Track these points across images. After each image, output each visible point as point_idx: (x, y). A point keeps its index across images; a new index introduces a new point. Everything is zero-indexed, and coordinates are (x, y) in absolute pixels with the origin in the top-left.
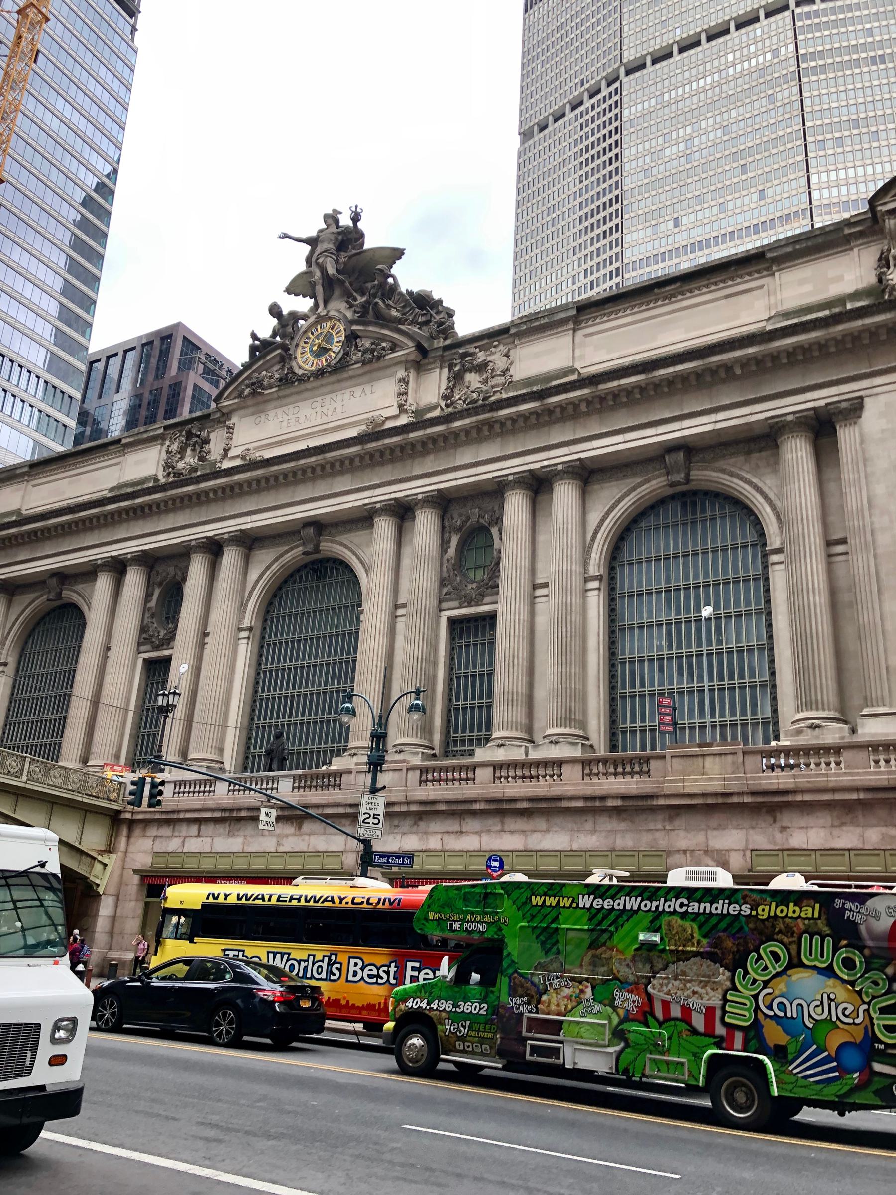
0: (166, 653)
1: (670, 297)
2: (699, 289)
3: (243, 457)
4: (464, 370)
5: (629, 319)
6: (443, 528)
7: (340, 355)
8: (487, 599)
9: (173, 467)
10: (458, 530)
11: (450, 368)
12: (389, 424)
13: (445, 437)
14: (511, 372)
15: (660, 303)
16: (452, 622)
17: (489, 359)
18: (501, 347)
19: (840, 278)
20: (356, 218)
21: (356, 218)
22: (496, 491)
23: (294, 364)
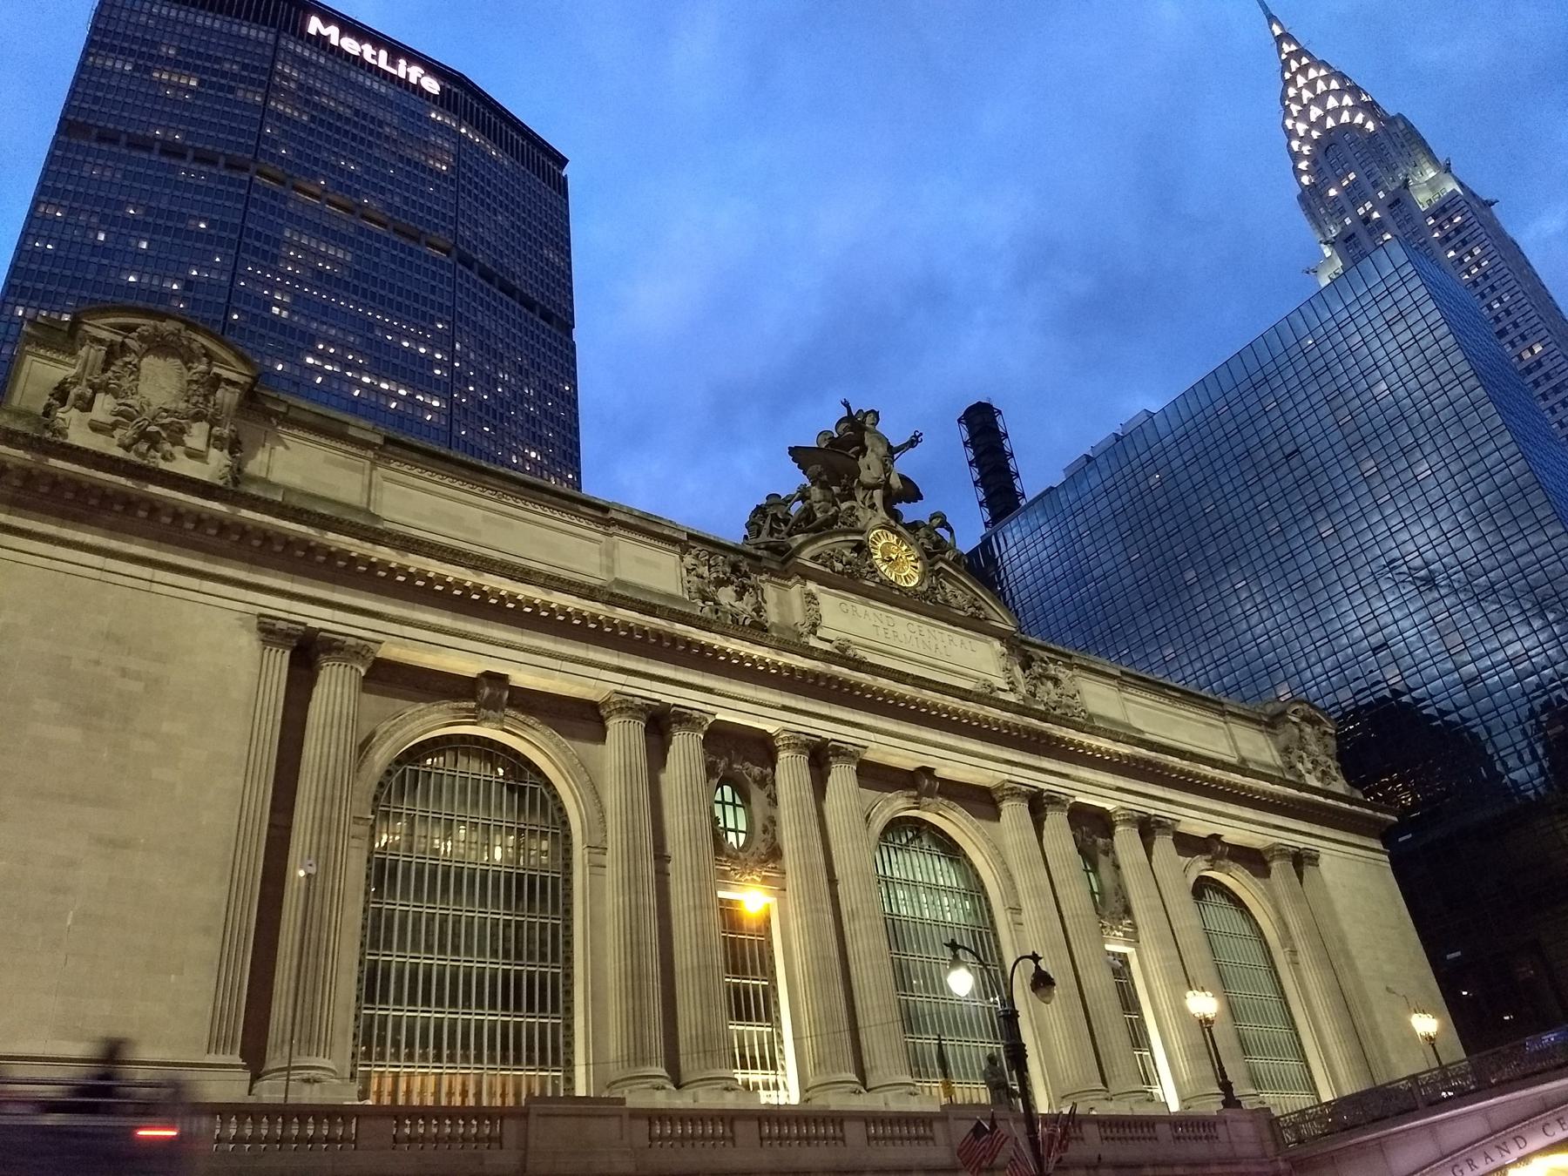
3: (843, 649)
7: (925, 587)
9: (717, 603)
17: (1061, 676)
20: (913, 442)
21: (913, 442)
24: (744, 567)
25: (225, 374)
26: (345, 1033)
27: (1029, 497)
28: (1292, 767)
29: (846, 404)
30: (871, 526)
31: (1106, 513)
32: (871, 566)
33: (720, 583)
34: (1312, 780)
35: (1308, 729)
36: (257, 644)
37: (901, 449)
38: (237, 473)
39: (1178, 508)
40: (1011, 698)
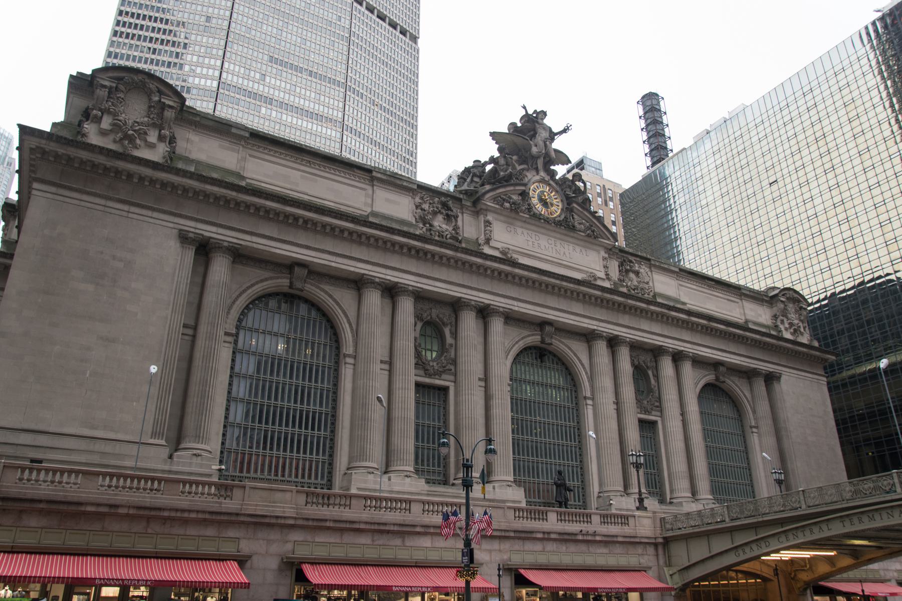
0: (438, 382)
5: (694, 287)
7: (563, 217)
8: (653, 413)
9: (431, 225)
12: (599, 283)
13: (642, 310)
14: (651, 284)
17: (642, 270)
19: (761, 316)
20: (565, 131)
21: (565, 131)
25: (167, 102)
26: (218, 434)
27: (675, 152)
28: (776, 326)
29: (524, 107)
30: (533, 181)
31: (712, 166)
32: (529, 205)
33: (435, 213)
34: (787, 335)
35: (791, 305)
36: (178, 245)
37: (561, 133)
38: (172, 155)
39: (753, 166)
40: (607, 284)
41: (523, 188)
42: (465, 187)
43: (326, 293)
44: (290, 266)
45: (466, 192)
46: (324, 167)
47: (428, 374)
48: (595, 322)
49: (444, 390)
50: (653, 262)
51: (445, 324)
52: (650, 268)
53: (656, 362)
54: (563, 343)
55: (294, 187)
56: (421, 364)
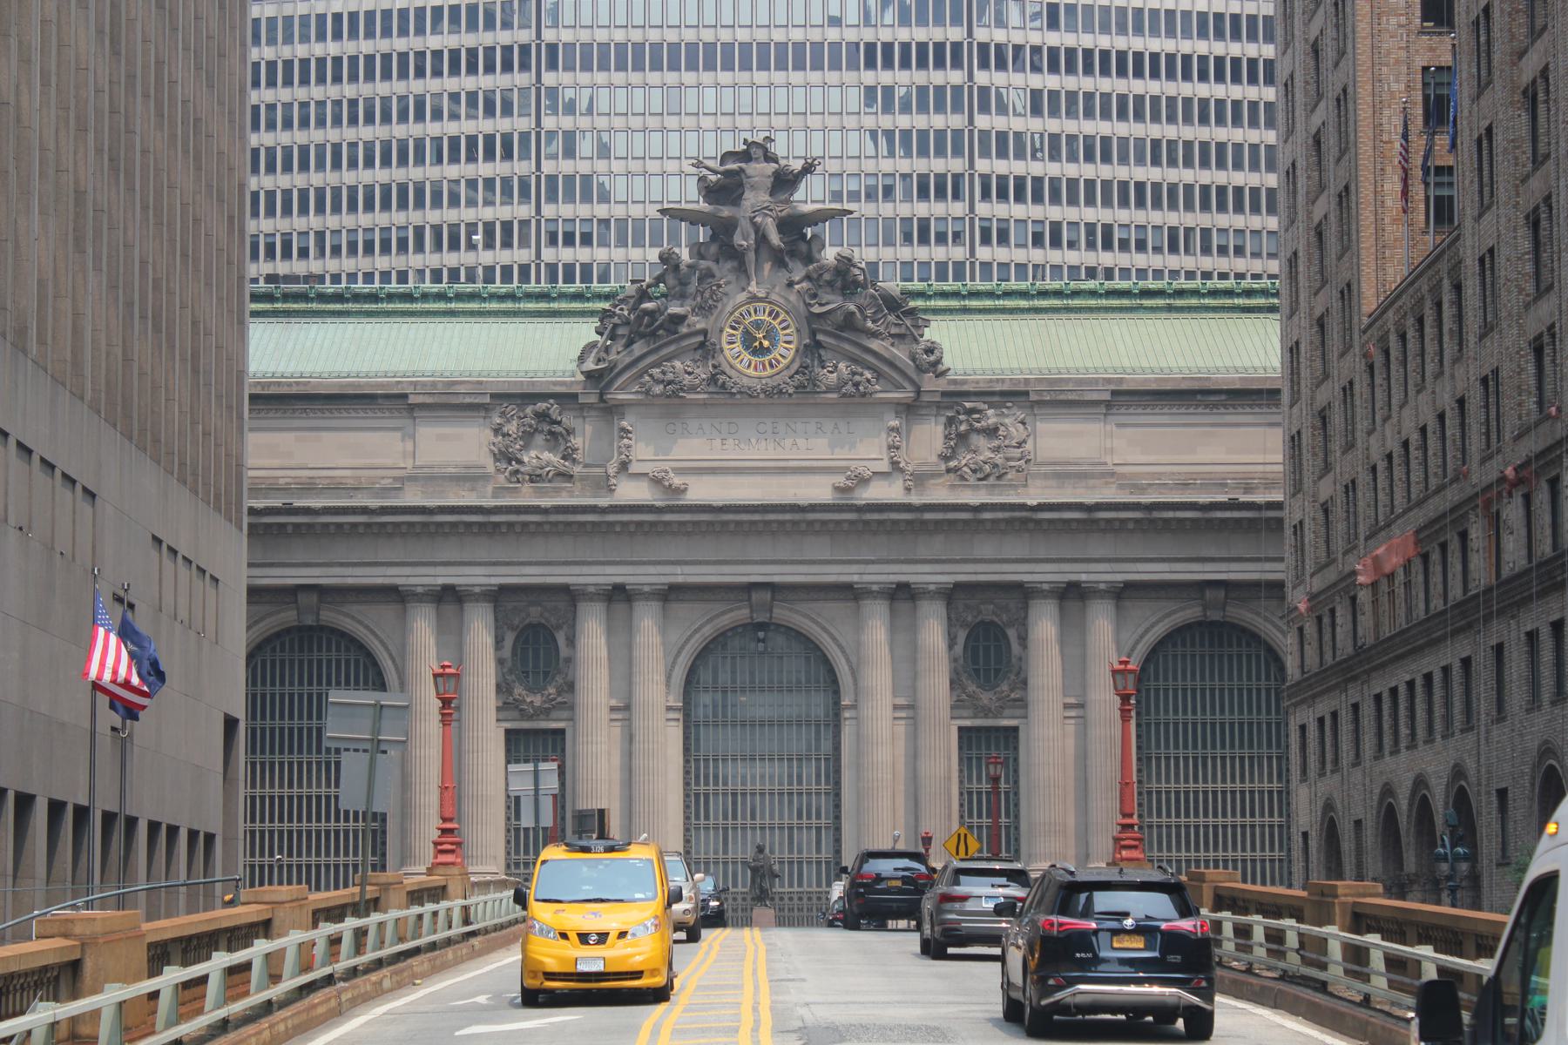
1: (1215, 406)
2: (1242, 406)
4: (972, 430)
6: (949, 618)
7: (796, 366)
8: (1007, 712)
9: (520, 462)
10: (964, 624)
11: (950, 422)
14: (1029, 446)
15: (1200, 410)
16: (960, 729)
18: (1014, 410)
20: (808, 169)
21: (808, 169)
22: (1023, 593)
23: (721, 358)
24: (555, 415)
33: (527, 437)
41: (701, 338)
42: (590, 365)
43: (353, 618)
44: (292, 593)
45: (589, 375)
46: (330, 411)
47: (523, 715)
48: (854, 568)
49: (562, 732)
50: (1033, 397)
51: (559, 627)
52: (1032, 407)
53: (1026, 608)
54: (797, 612)
55: (286, 463)
56: (508, 705)
